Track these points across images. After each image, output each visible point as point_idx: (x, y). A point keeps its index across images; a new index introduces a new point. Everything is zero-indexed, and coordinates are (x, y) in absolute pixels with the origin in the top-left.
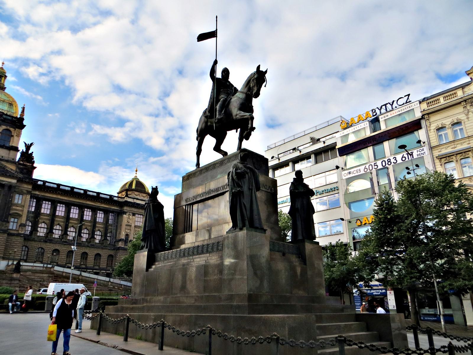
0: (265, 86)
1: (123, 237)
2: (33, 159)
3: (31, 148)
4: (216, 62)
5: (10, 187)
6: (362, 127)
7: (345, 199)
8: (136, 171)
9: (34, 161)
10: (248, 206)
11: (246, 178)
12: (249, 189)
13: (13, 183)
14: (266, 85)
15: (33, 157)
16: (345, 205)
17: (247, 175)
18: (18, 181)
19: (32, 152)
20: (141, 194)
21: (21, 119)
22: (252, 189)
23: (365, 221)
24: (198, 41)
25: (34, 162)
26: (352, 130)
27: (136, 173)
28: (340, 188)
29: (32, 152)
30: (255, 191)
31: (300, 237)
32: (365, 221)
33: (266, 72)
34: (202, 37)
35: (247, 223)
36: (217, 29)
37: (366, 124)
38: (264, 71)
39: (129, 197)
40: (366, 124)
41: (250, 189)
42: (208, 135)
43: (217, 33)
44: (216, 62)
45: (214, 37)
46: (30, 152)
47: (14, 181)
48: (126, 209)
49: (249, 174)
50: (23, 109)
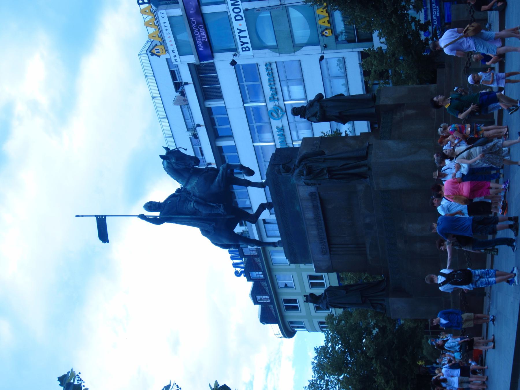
0: (186, 150)
6: (167, 21)
7: (286, 53)
10: (343, 162)
11: (311, 165)
12: (324, 161)
14: (185, 149)
16: (297, 53)
17: (308, 165)
22: (325, 159)
23: (324, 22)
24: (108, 242)
26: (169, 37)
28: (267, 60)
30: (325, 155)
31: (373, 110)
32: (324, 22)
34: (103, 236)
35: (362, 162)
36: (95, 216)
37: (163, 15)
40: (163, 15)
41: (325, 160)
42: (234, 230)
43: (99, 216)
45: (105, 219)
49: (307, 162)
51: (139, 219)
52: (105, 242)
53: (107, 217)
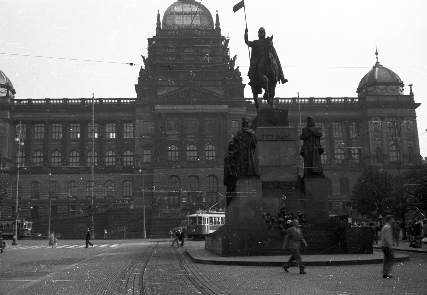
1: (373, 153)
2: (241, 75)
3: (235, 62)
4: (246, 31)
5: (224, 115)
8: (377, 54)
9: (241, 77)
13: (226, 109)
15: (240, 72)
18: (229, 106)
19: (238, 67)
20: (388, 88)
21: (218, 29)
22: (248, 148)
24: (234, 12)
25: (241, 79)
27: (377, 58)
29: (238, 67)
33: (272, 37)
34: (236, 8)
38: (270, 37)
39: (371, 96)
44: (246, 31)
46: (235, 68)
47: (226, 107)
48: (370, 112)
50: (217, 15)
51: (245, 29)
52: (233, 10)
53: (244, 7)
